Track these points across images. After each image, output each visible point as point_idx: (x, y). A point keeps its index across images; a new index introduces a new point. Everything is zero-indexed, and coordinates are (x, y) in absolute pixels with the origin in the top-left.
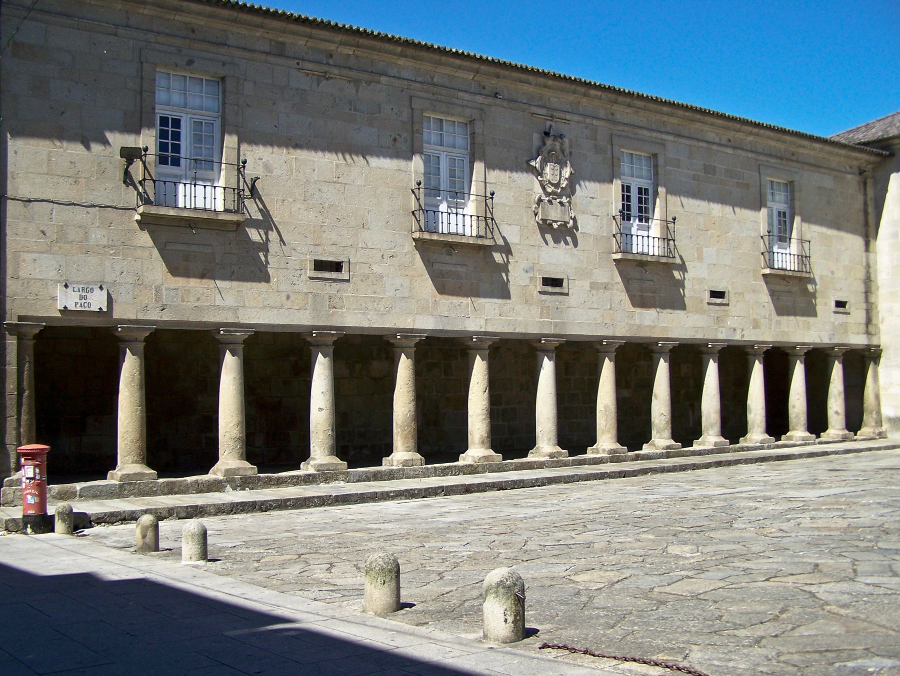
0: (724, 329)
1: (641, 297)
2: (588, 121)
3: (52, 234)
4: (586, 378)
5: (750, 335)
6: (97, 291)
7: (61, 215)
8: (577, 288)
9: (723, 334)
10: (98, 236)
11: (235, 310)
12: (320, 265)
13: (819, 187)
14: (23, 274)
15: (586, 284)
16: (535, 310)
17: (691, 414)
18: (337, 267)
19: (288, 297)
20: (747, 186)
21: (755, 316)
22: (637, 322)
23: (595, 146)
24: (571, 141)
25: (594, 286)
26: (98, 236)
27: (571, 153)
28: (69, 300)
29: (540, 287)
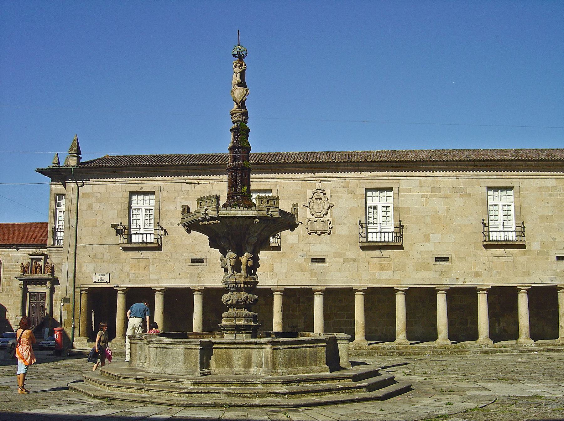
0: (448, 279)
1: (381, 264)
2: (342, 179)
3: (92, 255)
4: (412, 305)
5: (471, 282)
6: (106, 275)
7: (95, 248)
8: (334, 263)
9: (448, 282)
10: (107, 256)
11: (158, 280)
12: (194, 261)
13: (540, 187)
14: (83, 270)
15: (341, 260)
16: (307, 275)
17: (497, 325)
18: (201, 261)
19: (179, 274)
20: (470, 195)
21: (476, 270)
22: (377, 277)
23: (348, 190)
24: (331, 190)
25: (345, 261)
26: (107, 256)
27: (331, 196)
28: (96, 278)
29: (310, 263)
